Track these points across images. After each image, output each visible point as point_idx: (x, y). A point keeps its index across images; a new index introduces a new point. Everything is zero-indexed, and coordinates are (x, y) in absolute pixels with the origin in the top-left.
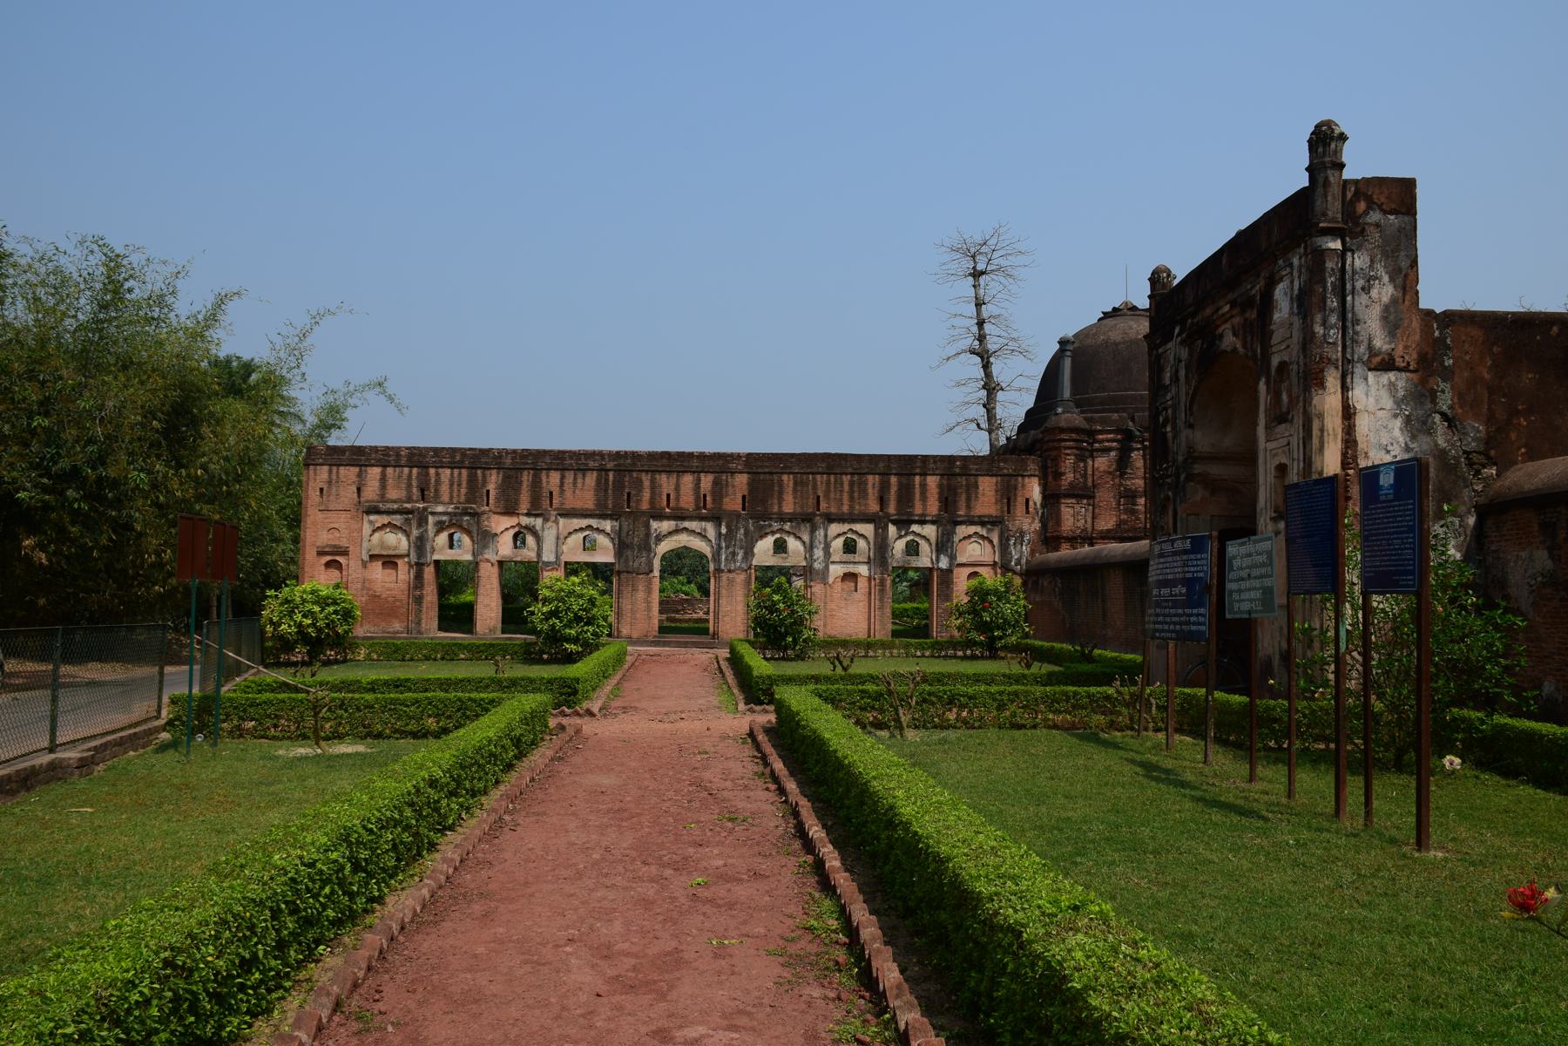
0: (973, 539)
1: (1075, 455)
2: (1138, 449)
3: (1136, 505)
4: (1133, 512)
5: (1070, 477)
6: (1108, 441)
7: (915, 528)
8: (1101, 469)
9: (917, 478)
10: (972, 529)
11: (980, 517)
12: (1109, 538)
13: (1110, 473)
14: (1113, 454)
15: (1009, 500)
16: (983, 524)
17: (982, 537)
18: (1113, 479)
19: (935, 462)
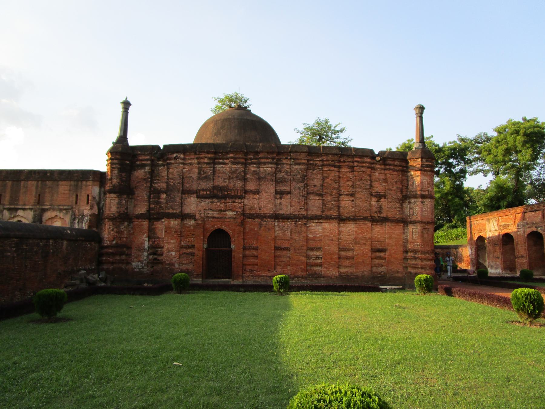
1: (118, 168)
3: (159, 198)
4: (158, 203)
5: (115, 181)
7: (20, 213)
8: (140, 177)
9: (23, 183)
10: (54, 214)
13: (144, 179)
14: (147, 169)
15: (77, 195)
16: (61, 210)
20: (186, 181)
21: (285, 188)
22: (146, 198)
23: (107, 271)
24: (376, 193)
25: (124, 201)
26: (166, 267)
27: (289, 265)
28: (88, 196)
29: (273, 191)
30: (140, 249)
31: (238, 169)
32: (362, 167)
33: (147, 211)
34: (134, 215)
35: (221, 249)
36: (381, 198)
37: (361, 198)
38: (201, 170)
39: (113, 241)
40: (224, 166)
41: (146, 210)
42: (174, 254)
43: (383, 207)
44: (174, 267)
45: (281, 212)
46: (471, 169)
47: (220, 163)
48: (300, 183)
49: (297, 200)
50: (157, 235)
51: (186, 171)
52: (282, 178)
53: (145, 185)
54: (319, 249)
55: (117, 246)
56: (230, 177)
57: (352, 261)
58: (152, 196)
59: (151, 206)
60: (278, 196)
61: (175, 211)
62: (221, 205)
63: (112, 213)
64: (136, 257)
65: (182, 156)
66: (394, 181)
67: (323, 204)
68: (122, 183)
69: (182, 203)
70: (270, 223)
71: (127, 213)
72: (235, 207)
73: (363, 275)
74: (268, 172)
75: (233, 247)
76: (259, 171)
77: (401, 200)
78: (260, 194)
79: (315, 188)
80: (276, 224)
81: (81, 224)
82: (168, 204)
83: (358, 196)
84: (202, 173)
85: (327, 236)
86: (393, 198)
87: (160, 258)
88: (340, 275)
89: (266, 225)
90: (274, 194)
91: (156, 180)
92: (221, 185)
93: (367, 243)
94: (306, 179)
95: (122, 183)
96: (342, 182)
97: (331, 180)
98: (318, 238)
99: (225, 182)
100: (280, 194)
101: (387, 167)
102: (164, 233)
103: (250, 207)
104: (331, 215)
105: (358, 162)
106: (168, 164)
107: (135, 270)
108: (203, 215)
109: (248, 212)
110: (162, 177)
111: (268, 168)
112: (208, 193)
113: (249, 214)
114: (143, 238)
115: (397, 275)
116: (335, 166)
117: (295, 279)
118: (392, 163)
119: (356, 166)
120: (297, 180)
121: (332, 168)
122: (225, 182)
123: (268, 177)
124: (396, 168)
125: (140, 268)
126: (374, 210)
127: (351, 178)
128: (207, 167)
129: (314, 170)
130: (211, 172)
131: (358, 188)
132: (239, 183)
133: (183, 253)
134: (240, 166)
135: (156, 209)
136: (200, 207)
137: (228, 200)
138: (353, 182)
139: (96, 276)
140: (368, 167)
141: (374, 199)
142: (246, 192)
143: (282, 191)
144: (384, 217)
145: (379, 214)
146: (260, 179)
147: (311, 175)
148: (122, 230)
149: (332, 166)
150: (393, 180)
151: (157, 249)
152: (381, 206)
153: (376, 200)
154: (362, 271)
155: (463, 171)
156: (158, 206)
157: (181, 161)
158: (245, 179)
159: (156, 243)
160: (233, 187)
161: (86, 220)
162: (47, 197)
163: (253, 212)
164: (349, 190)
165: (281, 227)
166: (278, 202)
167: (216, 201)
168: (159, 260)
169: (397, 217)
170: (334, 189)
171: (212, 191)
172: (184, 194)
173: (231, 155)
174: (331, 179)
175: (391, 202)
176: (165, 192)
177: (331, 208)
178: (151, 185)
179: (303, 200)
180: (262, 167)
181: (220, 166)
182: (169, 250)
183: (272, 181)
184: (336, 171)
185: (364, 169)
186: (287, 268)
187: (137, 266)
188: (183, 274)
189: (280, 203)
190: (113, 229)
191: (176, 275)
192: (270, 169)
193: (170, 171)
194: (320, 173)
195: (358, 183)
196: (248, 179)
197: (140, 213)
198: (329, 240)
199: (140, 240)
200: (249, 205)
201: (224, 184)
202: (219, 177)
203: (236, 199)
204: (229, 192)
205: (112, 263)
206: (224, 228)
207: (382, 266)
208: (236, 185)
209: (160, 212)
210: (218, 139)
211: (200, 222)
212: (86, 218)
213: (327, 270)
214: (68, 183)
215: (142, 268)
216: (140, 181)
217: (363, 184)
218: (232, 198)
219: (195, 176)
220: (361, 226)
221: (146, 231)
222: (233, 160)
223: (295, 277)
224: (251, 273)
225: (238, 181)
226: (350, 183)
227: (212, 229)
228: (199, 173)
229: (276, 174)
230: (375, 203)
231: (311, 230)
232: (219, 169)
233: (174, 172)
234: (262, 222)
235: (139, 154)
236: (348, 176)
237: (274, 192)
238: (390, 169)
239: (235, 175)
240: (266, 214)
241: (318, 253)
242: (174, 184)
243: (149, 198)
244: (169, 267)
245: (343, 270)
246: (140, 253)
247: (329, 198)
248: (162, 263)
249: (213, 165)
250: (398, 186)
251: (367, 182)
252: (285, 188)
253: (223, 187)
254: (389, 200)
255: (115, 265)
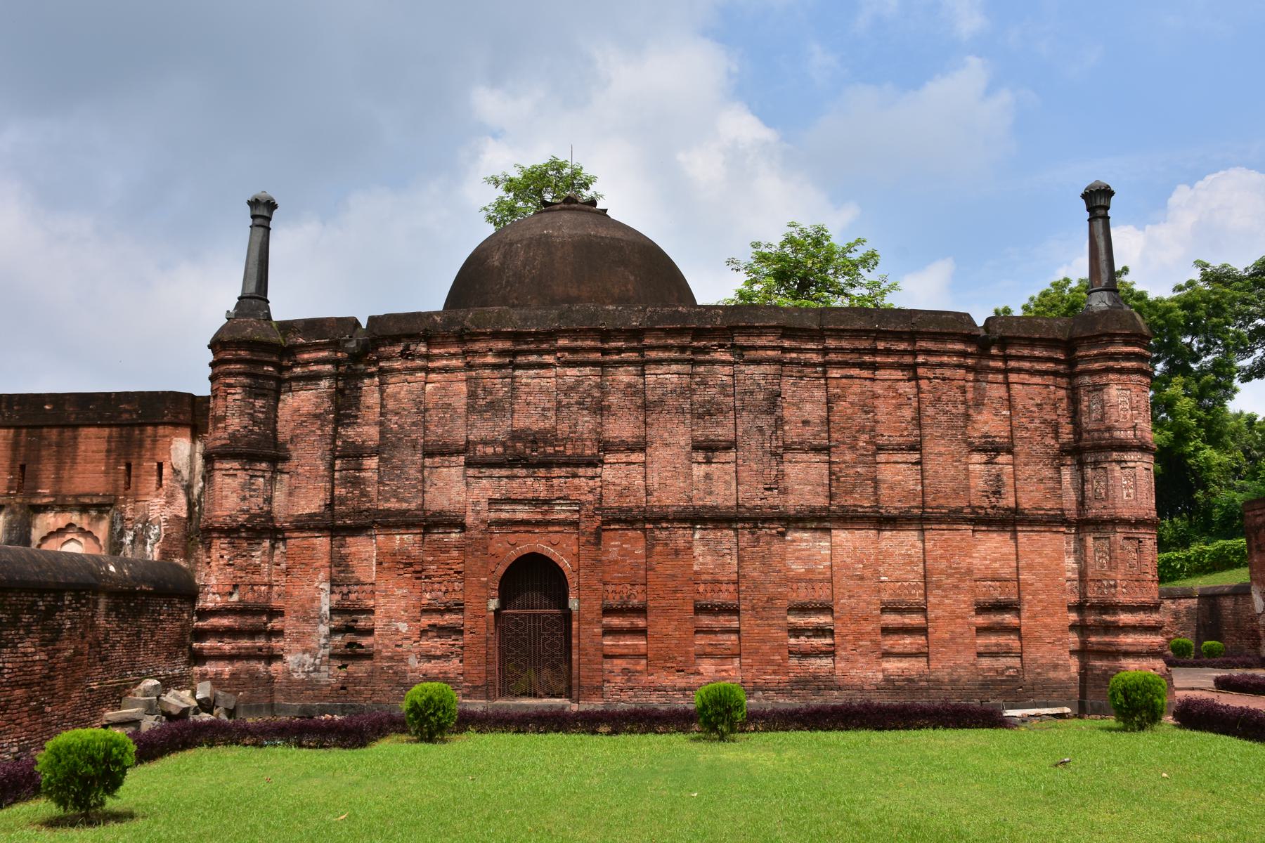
0: (68, 537)
1: (243, 386)
2: (371, 375)
3: (360, 470)
4: (356, 483)
5: (235, 423)
6: (318, 362)
8: (304, 411)
11: (76, 496)
12: (310, 529)
13: (316, 416)
14: (324, 384)
15: (129, 466)
16: (84, 509)
17: (82, 531)
18: (321, 428)
19: (9, 407)
20: (433, 416)
21: (720, 431)
22: (322, 468)
23: (217, 681)
24: (983, 440)
25: (261, 480)
26: (382, 668)
27: (739, 655)
28: (160, 466)
29: (684, 440)
30: (309, 615)
31: (582, 381)
32: (941, 365)
33: (326, 505)
34: (289, 520)
35: (538, 611)
36: (998, 454)
37: (940, 455)
38: (477, 386)
39: (231, 594)
40: (542, 372)
41: (322, 503)
42: (403, 627)
43: (1005, 478)
44: (407, 665)
45: (710, 501)
46: (1247, 362)
47: (530, 366)
48: (763, 416)
49: (755, 467)
50: (356, 575)
51: (435, 388)
52: (709, 402)
53: (319, 432)
54: (826, 609)
55: (241, 610)
56: (560, 402)
57: (921, 640)
58: (338, 462)
59: (337, 493)
60: (700, 457)
61: (405, 506)
62: (533, 485)
63: (228, 513)
64: (298, 641)
65: (423, 349)
66: (1032, 402)
67: (831, 473)
68: (256, 429)
69: (423, 481)
70: (681, 532)
71: (270, 512)
72: (578, 488)
73: (955, 677)
74: (670, 387)
75: (573, 604)
76: (644, 384)
77: (1056, 457)
78: (648, 450)
79: (807, 428)
80: (697, 536)
81: (141, 546)
82: (385, 485)
83: (930, 447)
84: (480, 393)
85: (847, 567)
86: (1033, 453)
87: (365, 641)
88: (887, 680)
89: (668, 538)
90: (689, 448)
91: (348, 416)
92: (535, 428)
93: (962, 585)
94: (778, 403)
95: (256, 429)
96: (883, 408)
97: (851, 403)
98: (820, 573)
99: (547, 418)
100: (707, 449)
101: (1013, 364)
102: (374, 568)
103: (619, 488)
104: (855, 506)
105: (928, 352)
106: (382, 372)
107: (295, 675)
108: (484, 515)
109: (611, 500)
110: (368, 407)
111: (667, 376)
112: (500, 450)
113: (620, 509)
114: (316, 584)
115: (1052, 675)
116: (862, 366)
117: (756, 695)
118: (1026, 352)
119: (924, 364)
120: (755, 406)
121: (855, 372)
122: (547, 418)
123: (671, 401)
124: (1038, 366)
125: (308, 672)
126: (979, 488)
127: (909, 399)
128: (494, 376)
129: (801, 378)
130: (506, 389)
131: (931, 426)
132: (586, 419)
133: (429, 625)
134: (587, 370)
135: (352, 499)
136: (476, 492)
137: (557, 471)
138: (919, 409)
139: (187, 693)
140: (959, 366)
141: (976, 457)
142: (606, 446)
143: (713, 441)
144: (1009, 509)
145: (993, 500)
146: (646, 407)
147: (794, 391)
148: (257, 561)
149: (854, 365)
150: (1032, 399)
151: (355, 617)
152: (998, 475)
153: (984, 458)
154: (951, 667)
155: (1223, 370)
156: (357, 492)
157: (419, 363)
158: (600, 409)
159: (353, 596)
160: (571, 433)
161: (155, 535)
162: (47, 472)
163: (629, 502)
164: (906, 433)
165: (712, 545)
166: (702, 474)
167: (522, 472)
168: (361, 646)
169: (1049, 506)
170: (862, 430)
171: (509, 443)
172: (428, 454)
173: (562, 342)
174: (850, 403)
175: (1026, 465)
176: (377, 451)
177: (855, 487)
178: (335, 430)
179: (774, 463)
180: (652, 372)
181: (532, 372)
182: (390, 617)
183: (680, 410)
184: (866, 379)
185: (948, 373)
186: (732, 664)
187: (299, 666)
188: (436, 685)
189: (708, 476)
190: (230, 560)
191: (417, 688)
192: (675, 378)
193: (388, 390)
194: (818, 387)
195: (930, 411)
196: (614, 408)
197: (307, 511)
198: (851, 577)
199: (308, 590)
200: (617, 481)
201: (541, 425)
202: (528, 404)
203: (578, 465)
204: (560, 446)
205: (231, 658)
206: (549, 551)
207: (1007, 653)
208: (580, 428)
209: (363, 508)
210: (515, 295)
211: (476, 534)
212: (154, 531)
213: (850, 666)
214: (106, 432)
215: (315, 670)
216: (305, 422)
217: (946, 413)
218: (567, 464)
219: (460, 402)
220: (943, 535)
221: (325, 561)
222: (567, 354)
223: (757, 688)
224: (629, 680)
225: (584, 416)
226: (908, 413)
227: (514, 554)
228: (472, 395)
229: (693, 391)
230: (982, 467)
231: (800, 550)
232: (529, 381)
233: (399, 393)
234: (657, 532)
235: (302, 345)
236: (900, 391)
237: (687, 445)
238: (1019, 371)
239: (575, 398)
240: (668, 507)
241: (822, 620)
242: (401, 427)
243: (332, 466)
244: (390, 668)
245: (893, 666)
246: (308, 629)
247: (848, 457)
248: (369, 656)
249: (510, 371)
250: (1048, 417)
251: (955, 407)
252: (720, 431)
253: (541, 432)
254: (1022, 458)
255: (239, 665)
